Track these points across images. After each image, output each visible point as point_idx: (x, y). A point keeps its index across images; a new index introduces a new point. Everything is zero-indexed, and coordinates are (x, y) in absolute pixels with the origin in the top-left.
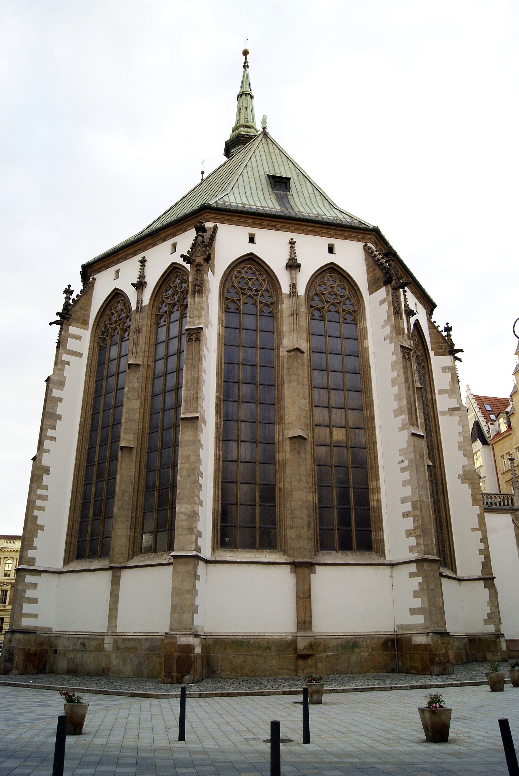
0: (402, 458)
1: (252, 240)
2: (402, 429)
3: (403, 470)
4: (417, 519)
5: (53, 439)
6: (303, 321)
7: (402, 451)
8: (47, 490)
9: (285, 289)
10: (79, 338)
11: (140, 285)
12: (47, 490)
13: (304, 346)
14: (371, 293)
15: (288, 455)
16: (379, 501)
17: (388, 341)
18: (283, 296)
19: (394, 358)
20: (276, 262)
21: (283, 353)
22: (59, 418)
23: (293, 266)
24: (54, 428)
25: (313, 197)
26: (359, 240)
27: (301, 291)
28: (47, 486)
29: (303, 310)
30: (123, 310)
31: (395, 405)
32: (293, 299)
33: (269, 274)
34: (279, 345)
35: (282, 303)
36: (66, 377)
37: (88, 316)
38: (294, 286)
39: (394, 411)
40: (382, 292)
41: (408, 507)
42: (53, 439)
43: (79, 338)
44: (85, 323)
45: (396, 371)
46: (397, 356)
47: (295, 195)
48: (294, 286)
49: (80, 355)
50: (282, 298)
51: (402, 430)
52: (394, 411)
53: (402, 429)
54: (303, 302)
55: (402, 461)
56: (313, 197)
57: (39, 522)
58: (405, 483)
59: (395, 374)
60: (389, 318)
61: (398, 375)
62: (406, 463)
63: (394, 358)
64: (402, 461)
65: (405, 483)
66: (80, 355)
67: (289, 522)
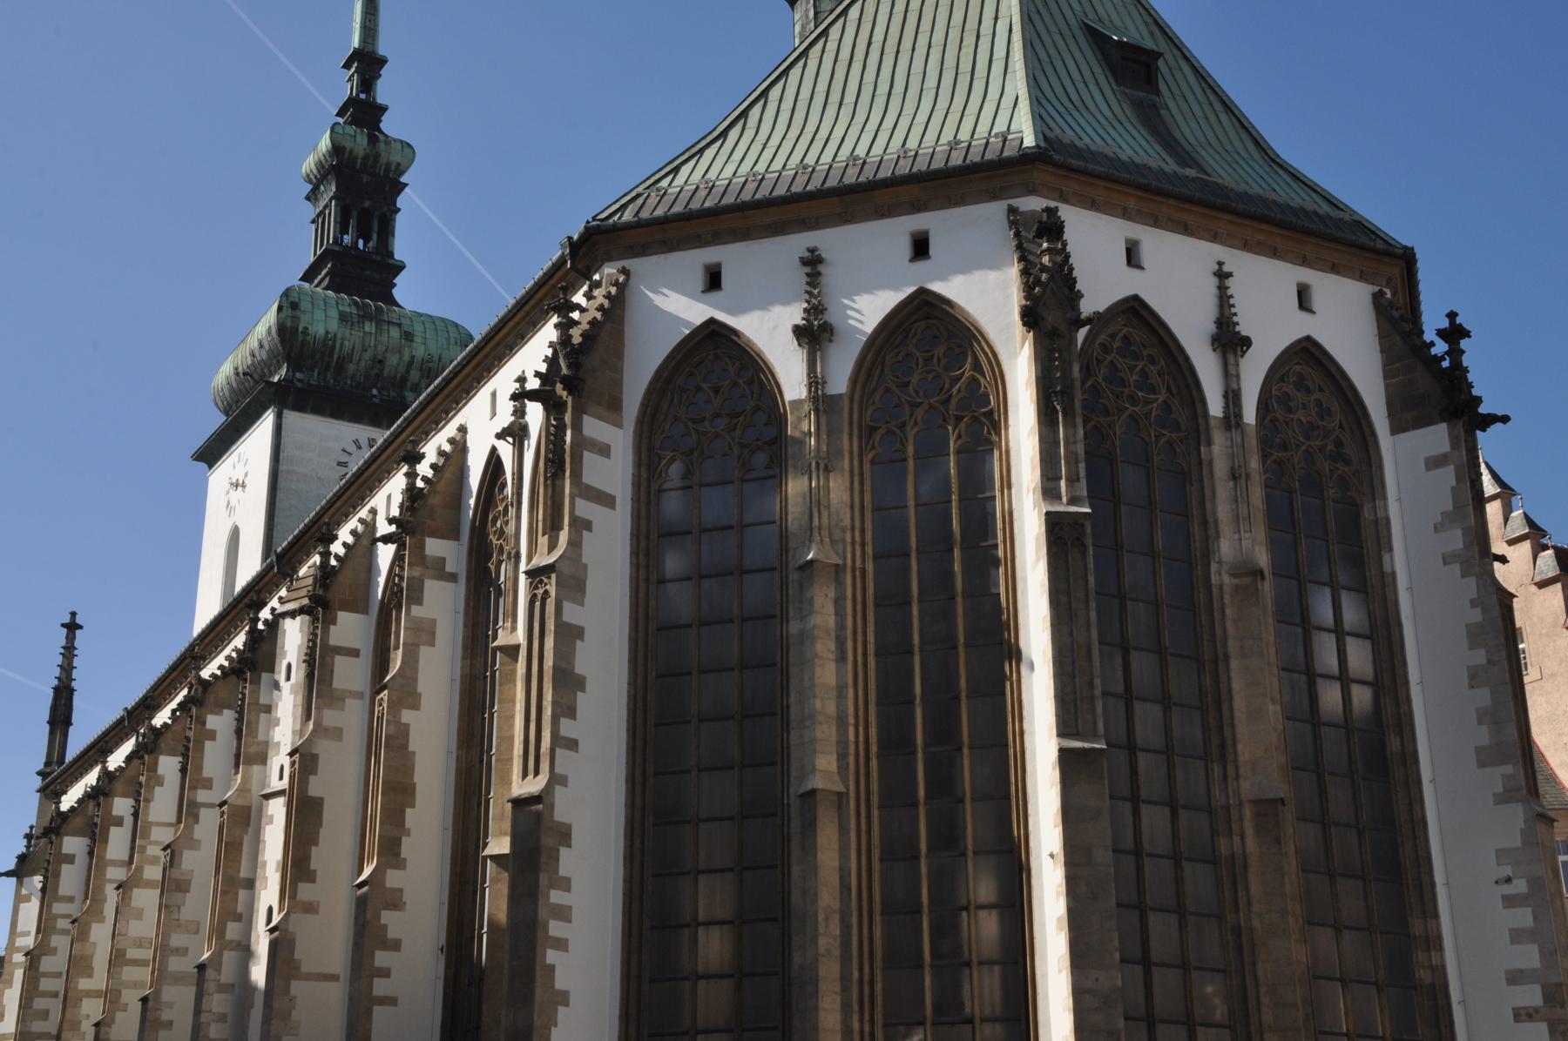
0: (1507, 871)
1: (1132, 256)
2: (1505, 798)
3: (1510, 901)
4: (1561, 1028)
5: (572, 744)
6: (1257, 494)
7: (1502, 855)
8: (568, 890)
9: (1215, 407)
10: (604, 450)
11: (814, 334)
12: (568, 890)
13: (1263, 559)
14: (1397, 428)
15: (1251, 845)
16: (1441, 971)
17: (1457, 567)
18: (1212, 423)
19: (1476, 616)
20: (1191, 326)
21: (1221, 578)
22: (579, 683)
23: (1229, 341)
24: (571, 713)
25: (1212, 117)
26: (1362, 277)
27: (1250, 415)
28: (568, 880)
29: (1254, 464)
30: (735, 384)
31: (1483, 736)
32: (1236, 434)
33: (1172, 355)
34: (1207, 555)
35: (1209, 443)
36: (585, 566)
37: (618, 384)
38: (1232, 397)
39: (1480, 751)
40: (1436, 438)
41: (1532, 996)
42: (572, 744)
43: (604, 450)
44: (612, 408)
45: (1482, 652)
46: (1485, 611)
47: (1171, 105)
48: (1232, 397)
49: (606, 500)
50: (1208, 428)
51: (1506, 801)
52: (1480, 751)
53: (1505, 798)
54: (1252, 442)
55: (1508, 880)
56: (1212, 117)
57: (560, 983)
58: (1517, 936)
59: (1480, 657)
60: (1458, 507)
61: (1489, 662)
62: (1520, 886)
63: (1476, 616)
64: (1508, 880)
65: (1517, 936)
66: (606, 500)
67: (1267, 1017)
